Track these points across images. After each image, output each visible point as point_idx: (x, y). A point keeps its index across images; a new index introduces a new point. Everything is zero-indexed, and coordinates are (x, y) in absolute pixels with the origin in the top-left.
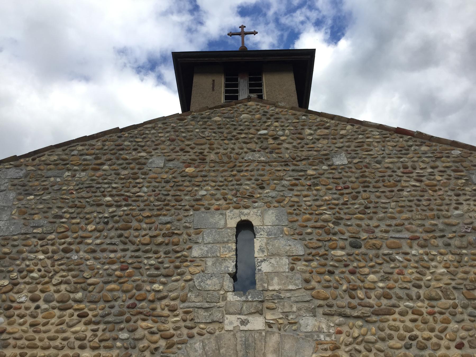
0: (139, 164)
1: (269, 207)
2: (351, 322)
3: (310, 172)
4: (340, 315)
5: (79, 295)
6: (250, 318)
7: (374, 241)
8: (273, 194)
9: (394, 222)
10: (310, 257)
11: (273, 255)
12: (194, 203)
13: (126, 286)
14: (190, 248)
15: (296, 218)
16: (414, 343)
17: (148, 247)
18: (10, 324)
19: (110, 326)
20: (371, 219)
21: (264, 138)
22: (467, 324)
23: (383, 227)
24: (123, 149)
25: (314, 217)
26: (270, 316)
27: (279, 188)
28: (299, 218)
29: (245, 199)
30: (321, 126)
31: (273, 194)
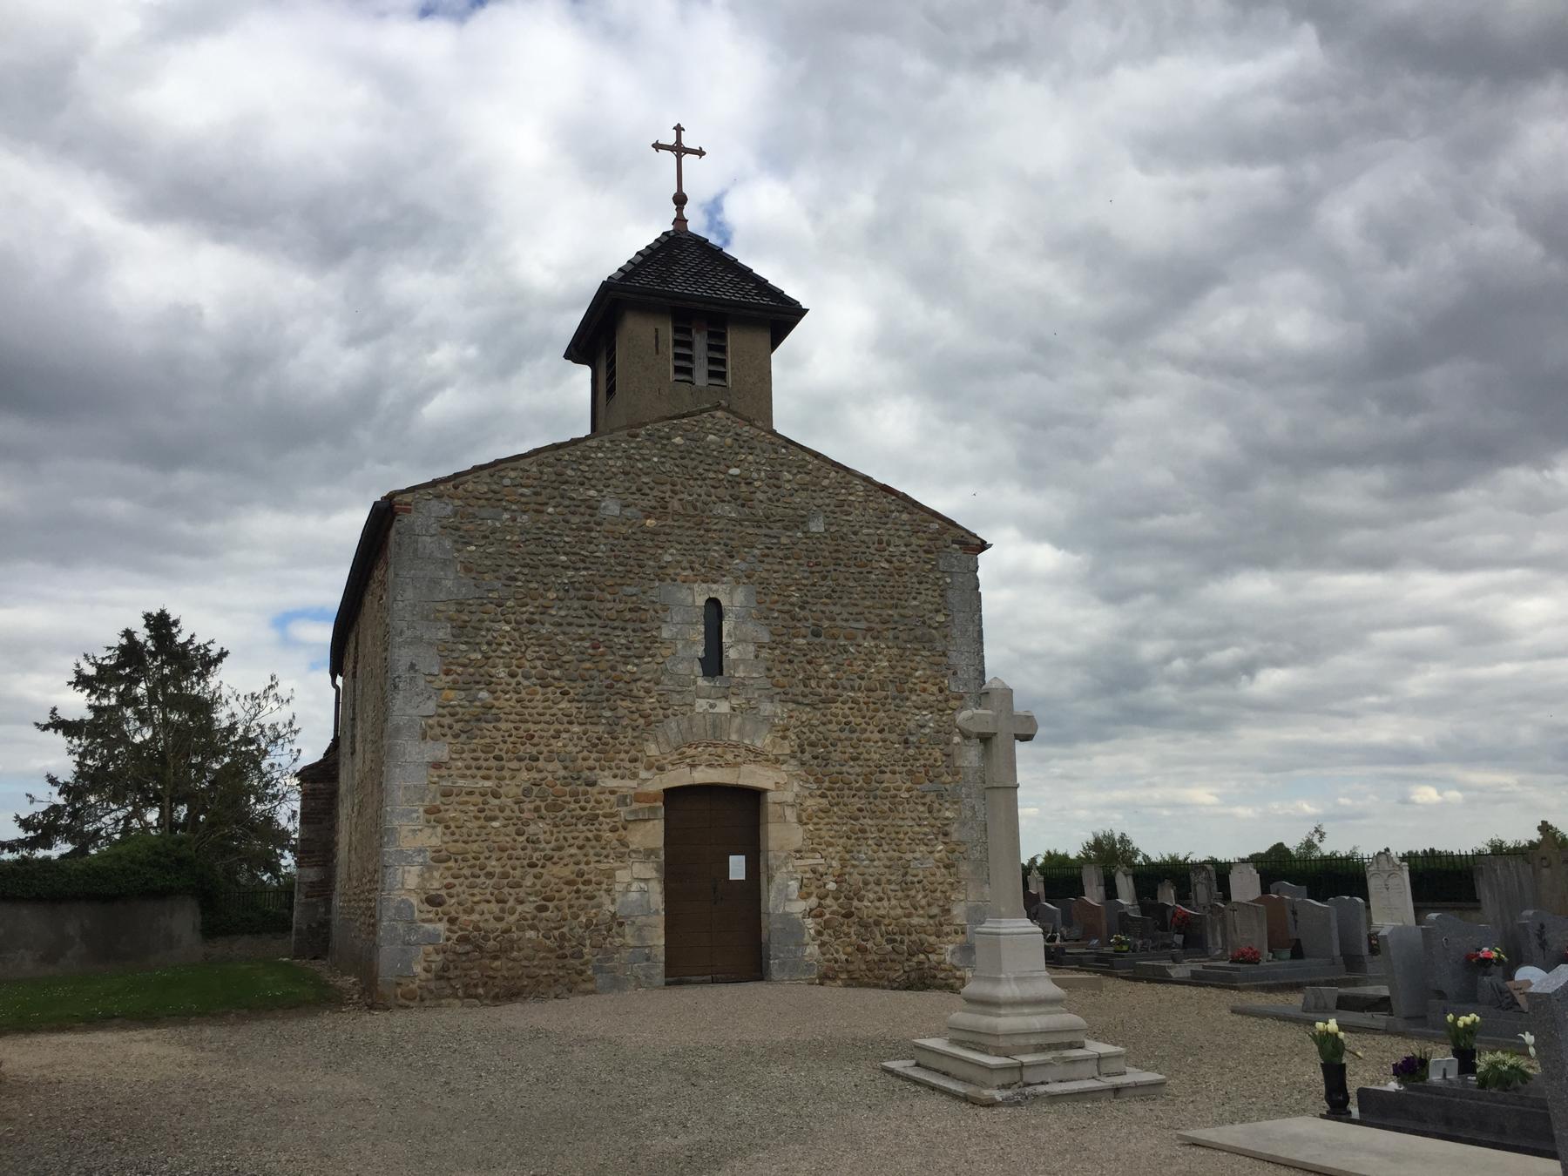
0: (589, 507)
3: (784, 540)
4: (794, 702)
5: (557, 673)
8: (743, 566)
9: (856, 610)
11: (739, 641)
13: (603, 665)
18: (497, 699)
21: (734, 482)
22: (892, 713)
23: (845, 616)
24: (566, 482)
26: (735, 702)
27: (749, 558)
29: (712, 572)
30: (802, 467)
31: (743, 566)
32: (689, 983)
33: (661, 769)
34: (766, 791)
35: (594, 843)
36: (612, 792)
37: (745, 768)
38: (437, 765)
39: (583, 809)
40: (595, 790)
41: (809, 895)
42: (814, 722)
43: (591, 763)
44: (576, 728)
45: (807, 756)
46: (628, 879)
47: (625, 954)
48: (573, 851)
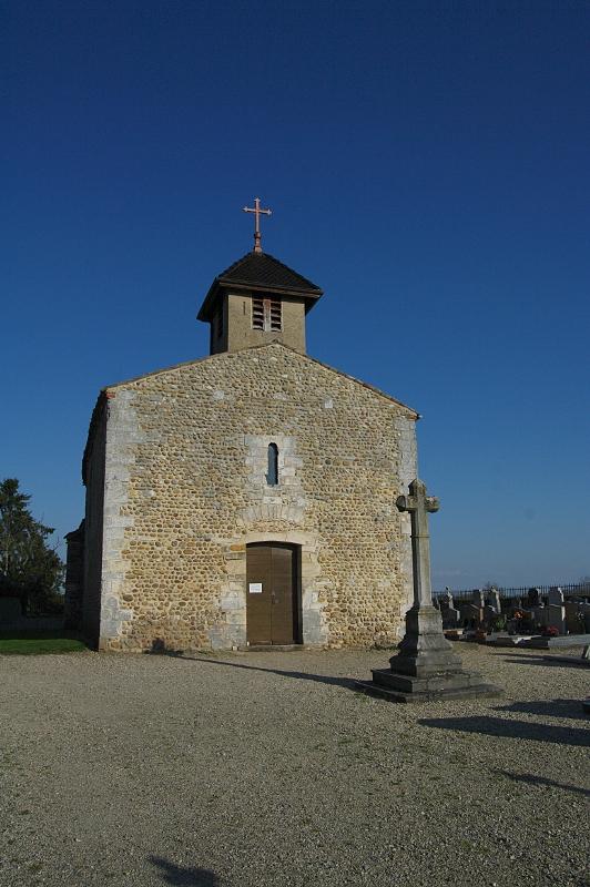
21: (284, 382)
22: (368, 505)
26: (285, 497)
29: (271, 429)
38: (127, 529)
45: (323, 527)
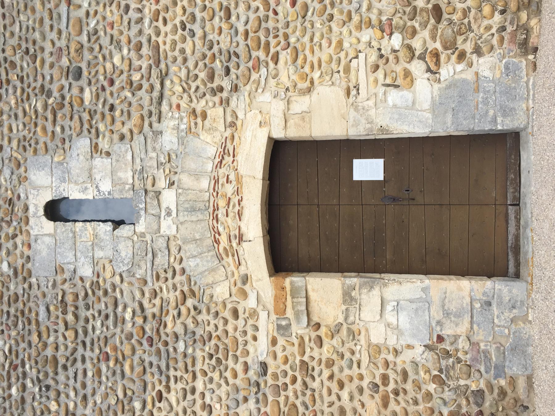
1: (26, 178)
2: (167, 93)
4: (160, 104)
6: (164, 206)
7: (72, 50)
10: (93, 131)
12: (20, 277)
13: (127, 351)
14: (82, 279)
15: (41, 145)
16: (188, 26)
17: (80, 331)
19: (171, 363)
20: (42, 49)
23: (54, 35)
25: (40, 122)
26: (162, 183)
28: (42, 140)
32: (517, 238)
33: (245, 279)
34: (270, 139)
35: (336, 369)
36: (274, 342)
37: (242, 171)
39: (294, 380)
40: (270, 362)
41: (407, 74)
42: (183, 74)
43: (239, 368)
44: (199, 385)
45: (226, 84)
46: (382, 327)
47: (480, 336)
48: (345, 395)
